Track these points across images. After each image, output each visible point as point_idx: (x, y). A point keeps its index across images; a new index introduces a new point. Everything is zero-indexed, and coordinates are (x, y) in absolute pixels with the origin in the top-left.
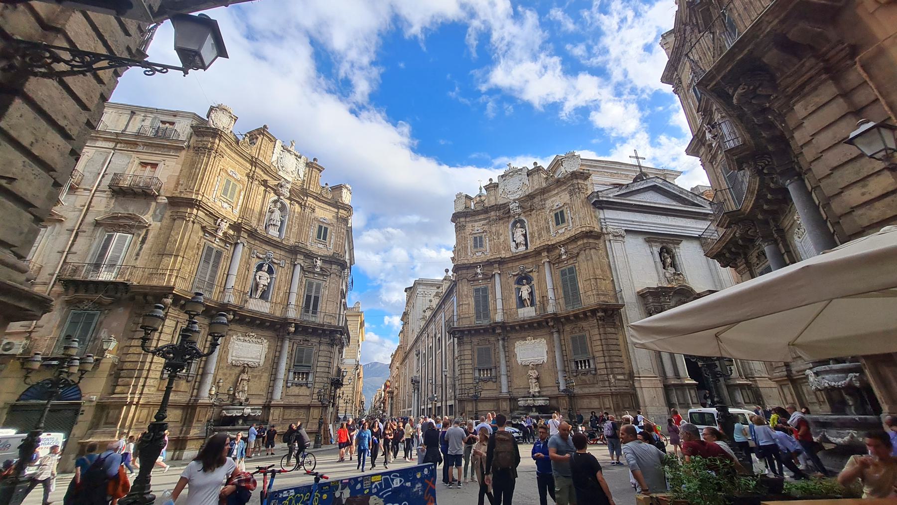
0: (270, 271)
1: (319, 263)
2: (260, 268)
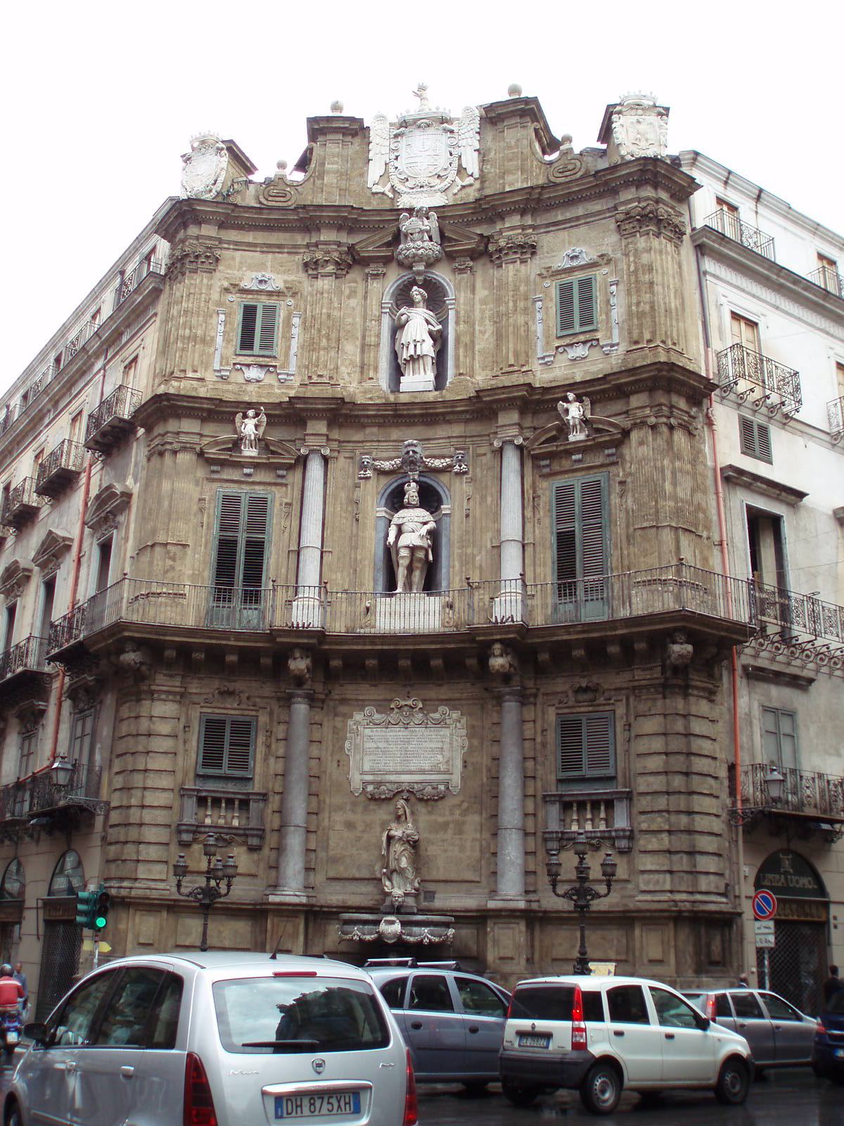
0: (430, 499)
1: (575, 411)
2: (396, 501)
